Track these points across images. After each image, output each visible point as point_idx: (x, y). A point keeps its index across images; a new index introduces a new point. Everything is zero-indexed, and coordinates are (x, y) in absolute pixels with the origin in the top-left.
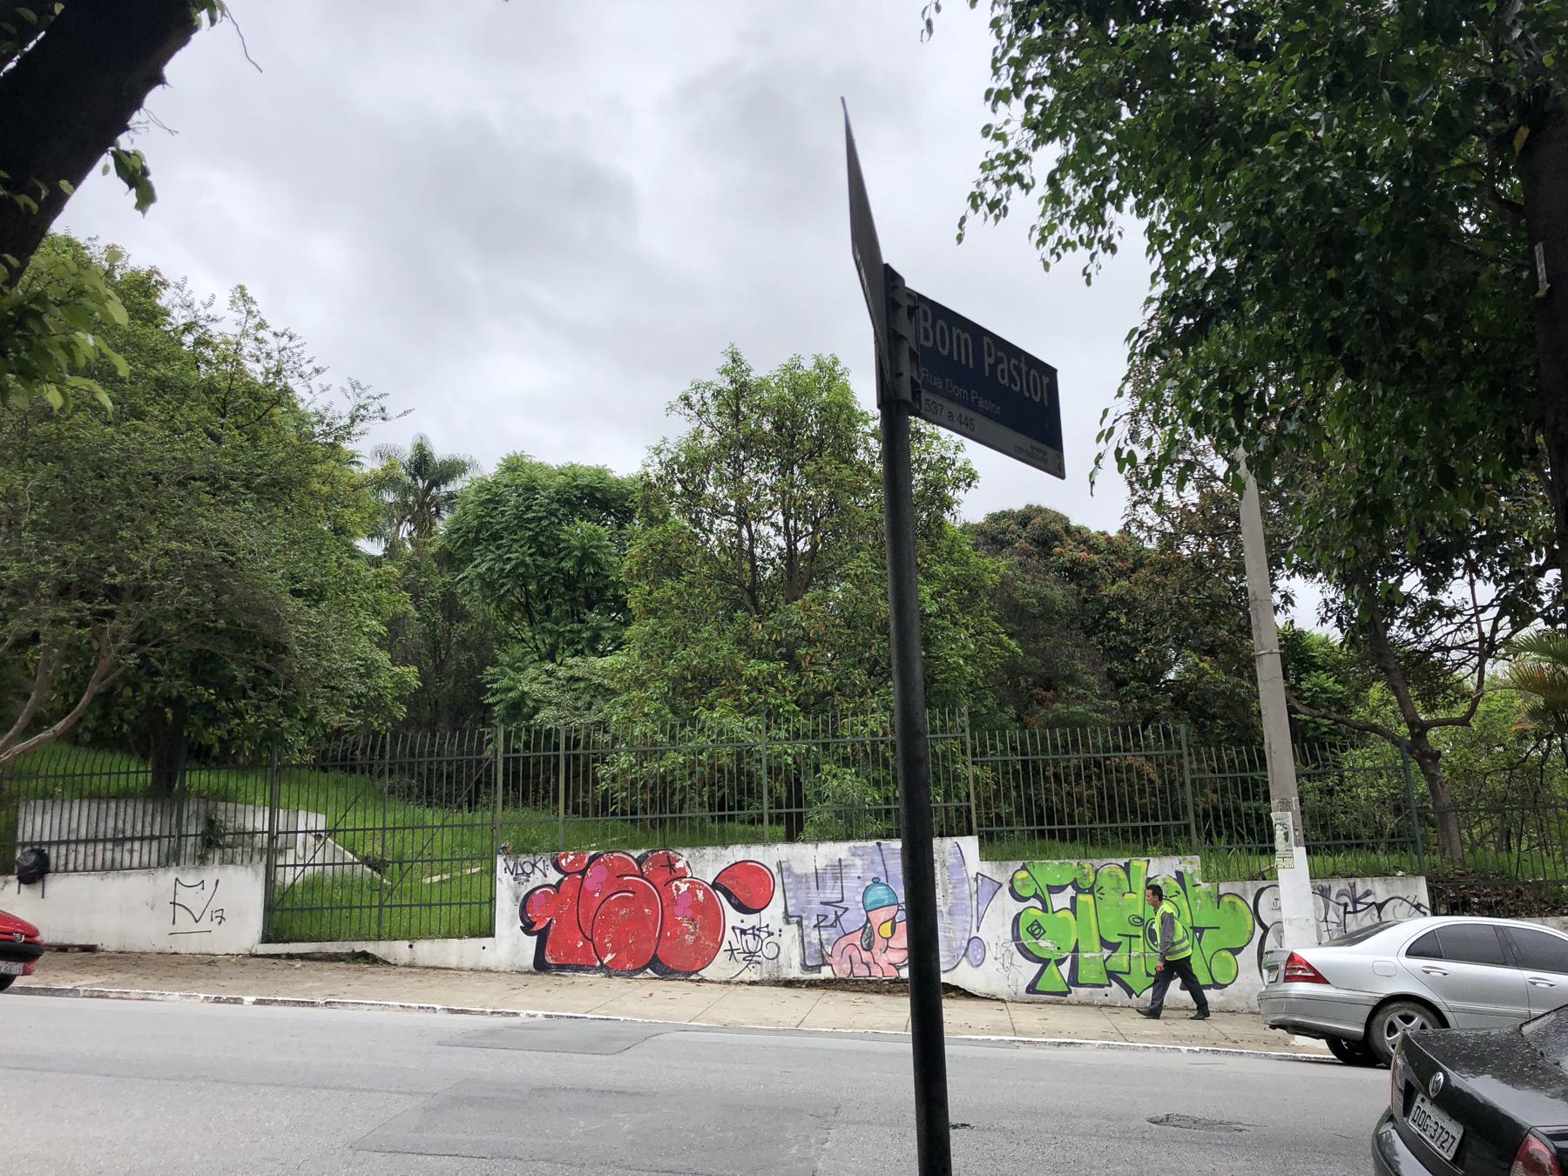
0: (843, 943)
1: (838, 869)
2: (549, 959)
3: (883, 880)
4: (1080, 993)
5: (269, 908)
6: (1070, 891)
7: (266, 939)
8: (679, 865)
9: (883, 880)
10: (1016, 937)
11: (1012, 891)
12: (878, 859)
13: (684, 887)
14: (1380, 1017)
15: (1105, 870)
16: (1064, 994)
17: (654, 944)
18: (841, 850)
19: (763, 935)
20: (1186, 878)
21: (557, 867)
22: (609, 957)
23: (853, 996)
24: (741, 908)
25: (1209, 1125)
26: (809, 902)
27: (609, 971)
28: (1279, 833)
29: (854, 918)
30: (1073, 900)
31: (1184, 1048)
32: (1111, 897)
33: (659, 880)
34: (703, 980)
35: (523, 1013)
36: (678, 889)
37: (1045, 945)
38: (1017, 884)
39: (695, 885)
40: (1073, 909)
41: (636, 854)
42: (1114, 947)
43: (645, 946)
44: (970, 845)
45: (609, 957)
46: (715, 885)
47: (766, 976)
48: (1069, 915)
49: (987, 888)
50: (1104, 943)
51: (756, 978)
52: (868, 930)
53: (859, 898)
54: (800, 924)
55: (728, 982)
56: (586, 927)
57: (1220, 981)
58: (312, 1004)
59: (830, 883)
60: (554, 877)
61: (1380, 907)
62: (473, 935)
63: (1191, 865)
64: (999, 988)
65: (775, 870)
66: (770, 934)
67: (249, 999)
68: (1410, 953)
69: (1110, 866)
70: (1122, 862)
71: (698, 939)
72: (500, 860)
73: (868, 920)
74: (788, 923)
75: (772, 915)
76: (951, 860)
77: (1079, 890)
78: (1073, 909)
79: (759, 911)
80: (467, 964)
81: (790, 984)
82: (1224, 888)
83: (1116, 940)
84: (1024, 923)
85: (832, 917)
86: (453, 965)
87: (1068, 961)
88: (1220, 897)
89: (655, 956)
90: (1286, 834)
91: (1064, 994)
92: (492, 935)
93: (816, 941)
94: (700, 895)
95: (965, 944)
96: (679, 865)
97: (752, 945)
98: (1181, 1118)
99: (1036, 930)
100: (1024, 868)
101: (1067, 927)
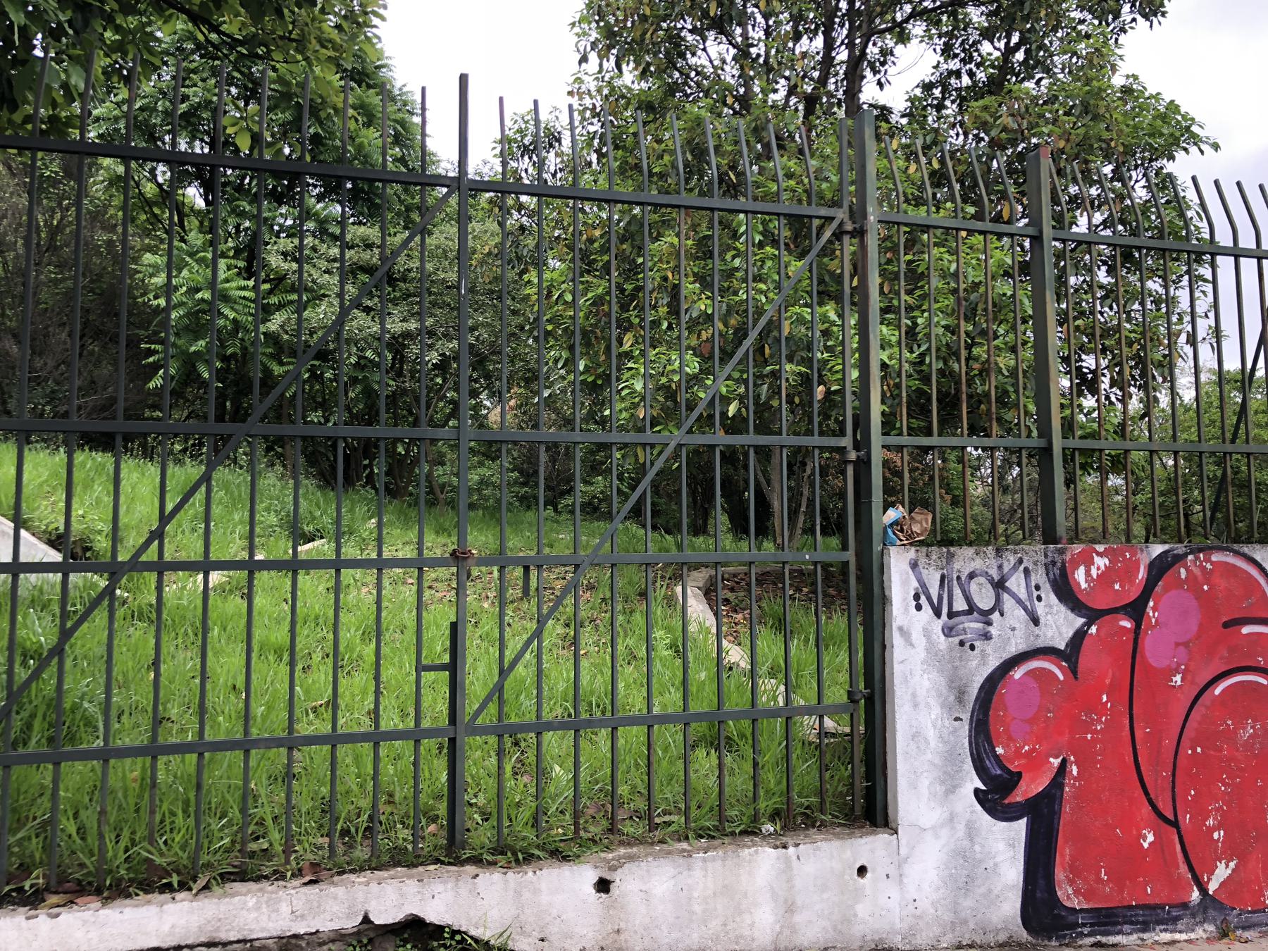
2: (1068, 895)
21: (1065, 591)
22: (1222, 872)
45: (1222, 872)
56: (1157, 778)
60: (1059, 625)
62: (793, 820)
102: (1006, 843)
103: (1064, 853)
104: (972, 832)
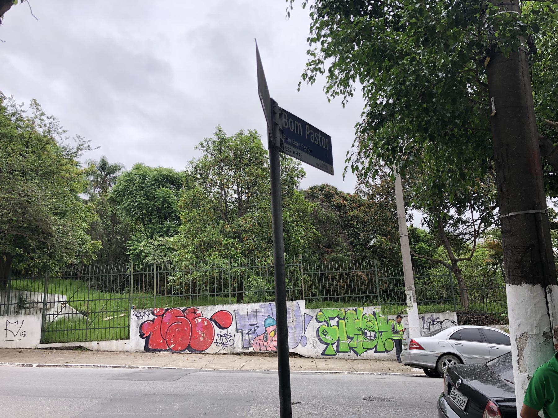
0: (257, 339)
1: (256, 313)
2: (150, 347)
3: (271, 316)
4: (340, 355)
5: (43, 331)
6: (337, 319)
7: (42, 342)
8: (198, 312)
9: (271, 316)
10: (318, 336)
11: (317, 319)
12: (270, 309)
13: (200, 320)
14: (441, 361)
15: (349, 312)
16: (334, 355)
17: (188, 341)
18: (256, 306)
19: (228, 337)
20: (377, 314)
21: (153, 314)
22: (172, 346)
23: (260, 358)
24: (221, 327)
25: (383, 400)
26: (245, 325)
27: (172, 351)
28: (408, 298)
30: (338, 322)
31: (375, 373)
32: (351, 321)
33: (191, 318)
34: (206, 353)
35: (140, 367)
36: (197, 321)
37: (328, 338)
38: (318, 317)
39: (204, 319)
40: (338, 325)
41: (182, 309)
42: (352, 338)
43: (185, 342)
44: (302, 303)
45: (172, 346)
46: (211, 319)
47: (229, 351)
48: (336, 327)
49: (308, 318)
50: (348, 337)
51: (226, 352)
52: (266, 334)
53: (263, 323)
54: (242, 333)
55: (215, 354)
56: (164, 335)
57: (388, 349)
58: (60, 366)
59: (252, 318)
60: (152, 317)
61: (441, 323)
63: (378, 309)
64: (312, 353)
65: (233, 313)
66: (231, 336)
67: (35, 365)
68: (451, 338)
69: (350, 310)
70: (354, 308)
71: (205, 339)
72: (132, 311)
73: (266, 331)
74: (237, 332)
75: (232, 329)
76: (295, 309)
77: (340, 319)
78: (338, 325)
79: (227, 328)
80: (120, 349)
81: (238, 354)
82: (389, 317)
83: (352, 336)
84: (321, 330)
85: (253, 330)
86: (114, 350)
87: (336, 344)
88: (388, 320)
89: (189, 345)
90: (410, 298)
91: (334, 355)
92: (129, 339)
93: (247, 339)
94: (206, 323)
95: (300, 338)
96: (198, 312)
97: (224, 341)
98: (374, 397)
99: (325, 333)
100: (321, 311)
101: (335, 332)
102: (143, 341)
103: (150, 342)
104: (139, 340)
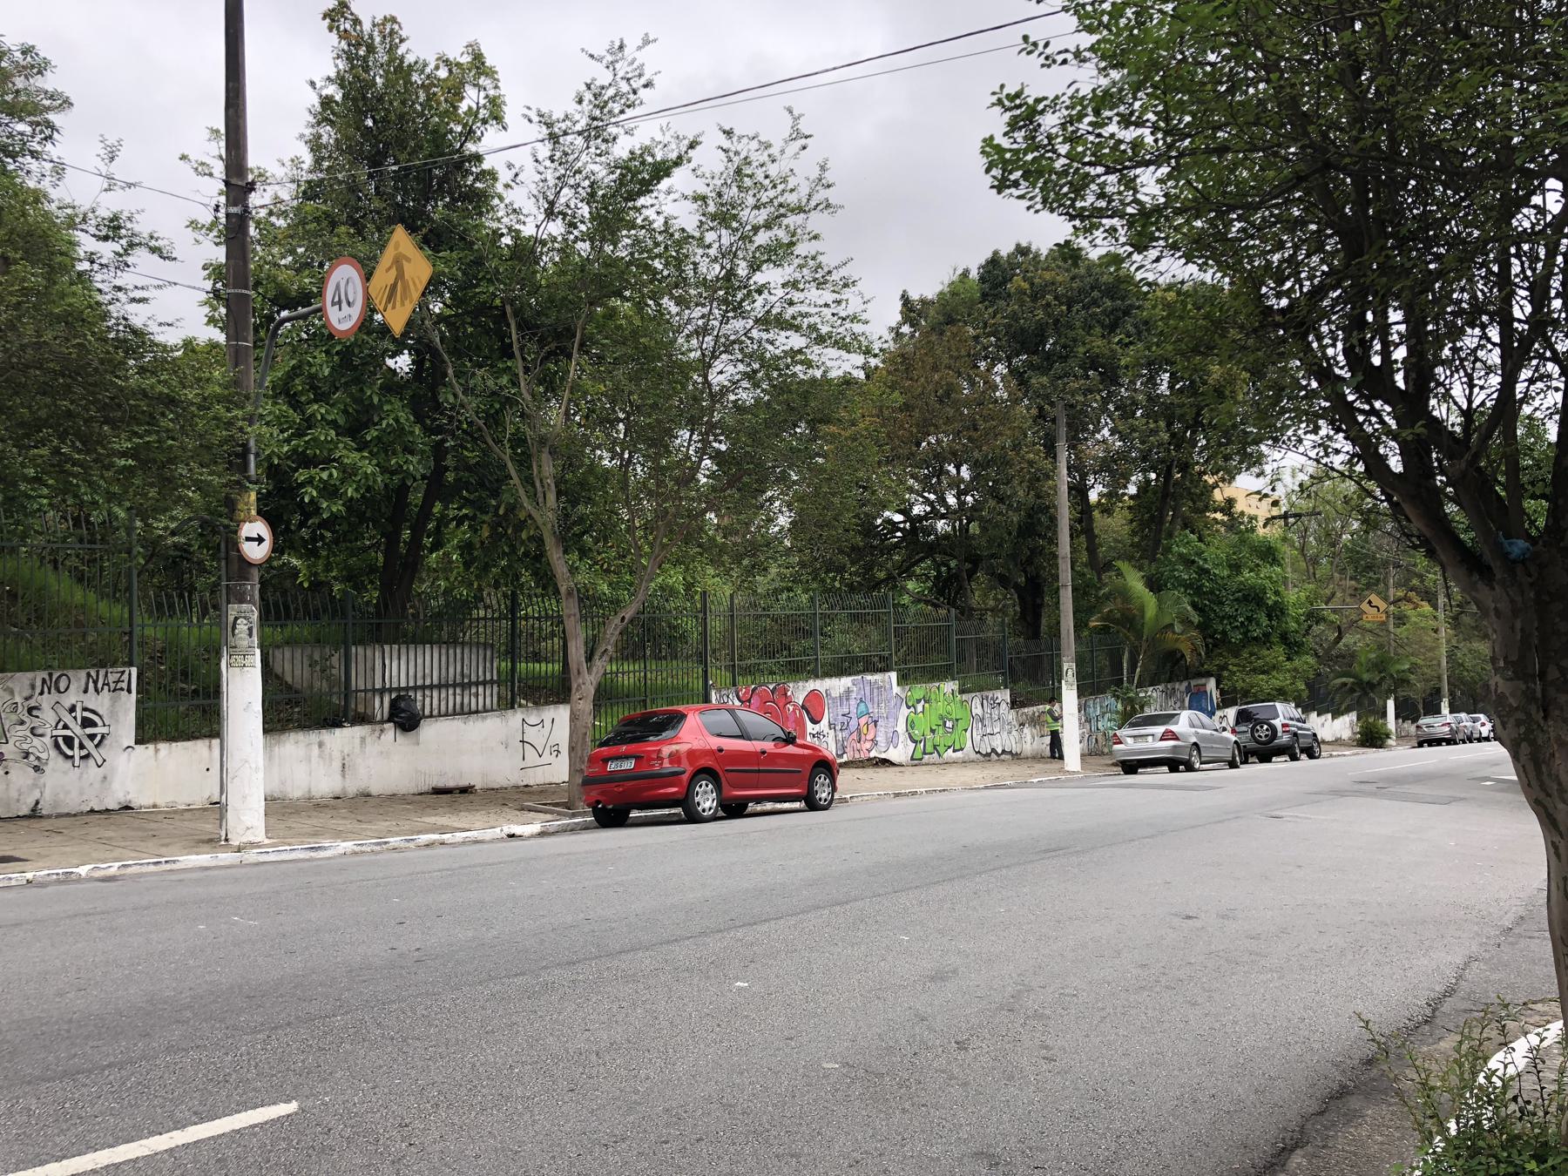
18: (846, 682)
29: (854, 723)
52: (859, 730)
